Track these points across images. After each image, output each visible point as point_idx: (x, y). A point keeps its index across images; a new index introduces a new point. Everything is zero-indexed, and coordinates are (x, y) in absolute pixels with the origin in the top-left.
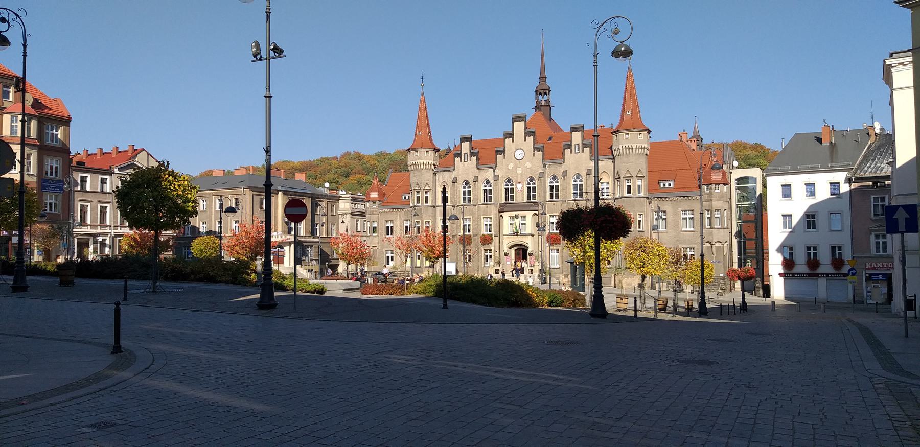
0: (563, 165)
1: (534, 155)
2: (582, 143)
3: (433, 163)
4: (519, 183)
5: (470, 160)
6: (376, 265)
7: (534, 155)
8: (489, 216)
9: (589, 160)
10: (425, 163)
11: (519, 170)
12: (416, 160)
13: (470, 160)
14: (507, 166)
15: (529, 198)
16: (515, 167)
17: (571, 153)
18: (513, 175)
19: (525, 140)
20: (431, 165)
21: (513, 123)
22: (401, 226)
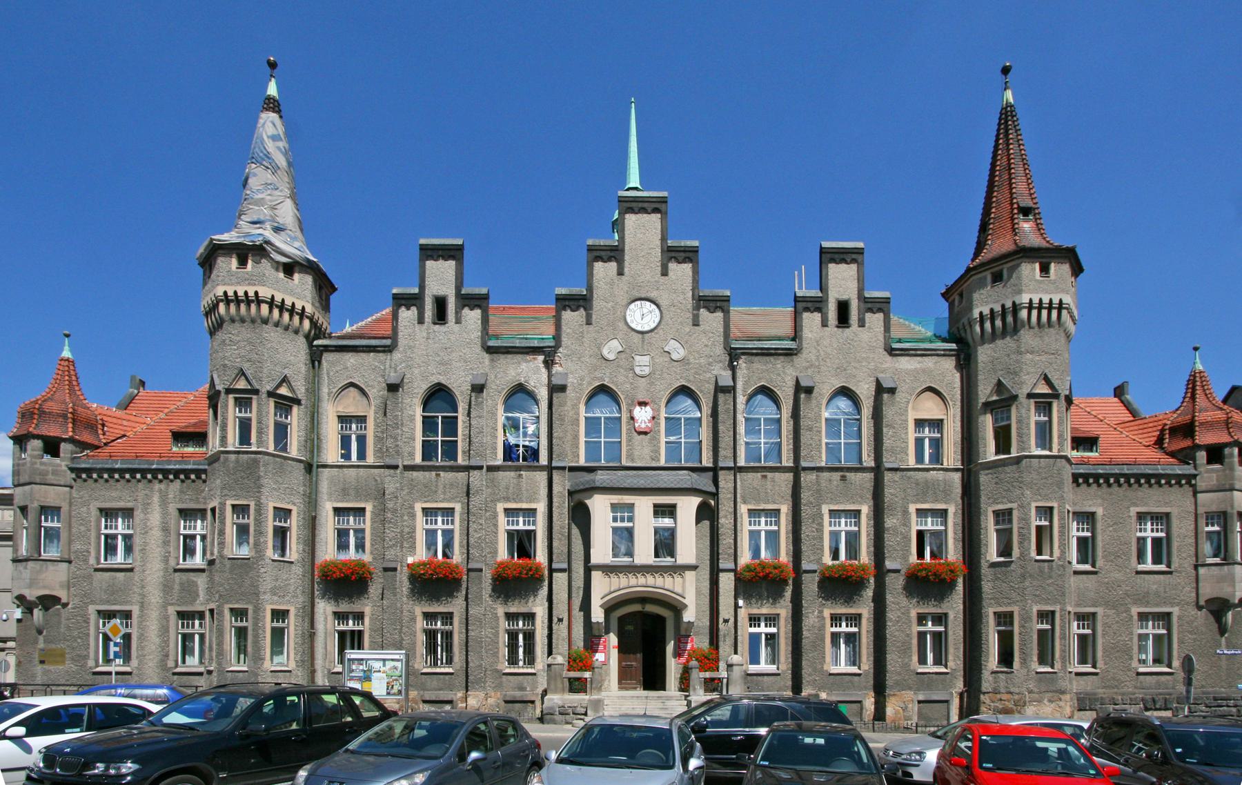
0: (799, 361)
4: (643, 404)
6: (56, 663)
9: (882, 350)
11: (643, 364)
16: (627, 354)
18: (621, 379)
19: (665, 273)
22: (165, 529)
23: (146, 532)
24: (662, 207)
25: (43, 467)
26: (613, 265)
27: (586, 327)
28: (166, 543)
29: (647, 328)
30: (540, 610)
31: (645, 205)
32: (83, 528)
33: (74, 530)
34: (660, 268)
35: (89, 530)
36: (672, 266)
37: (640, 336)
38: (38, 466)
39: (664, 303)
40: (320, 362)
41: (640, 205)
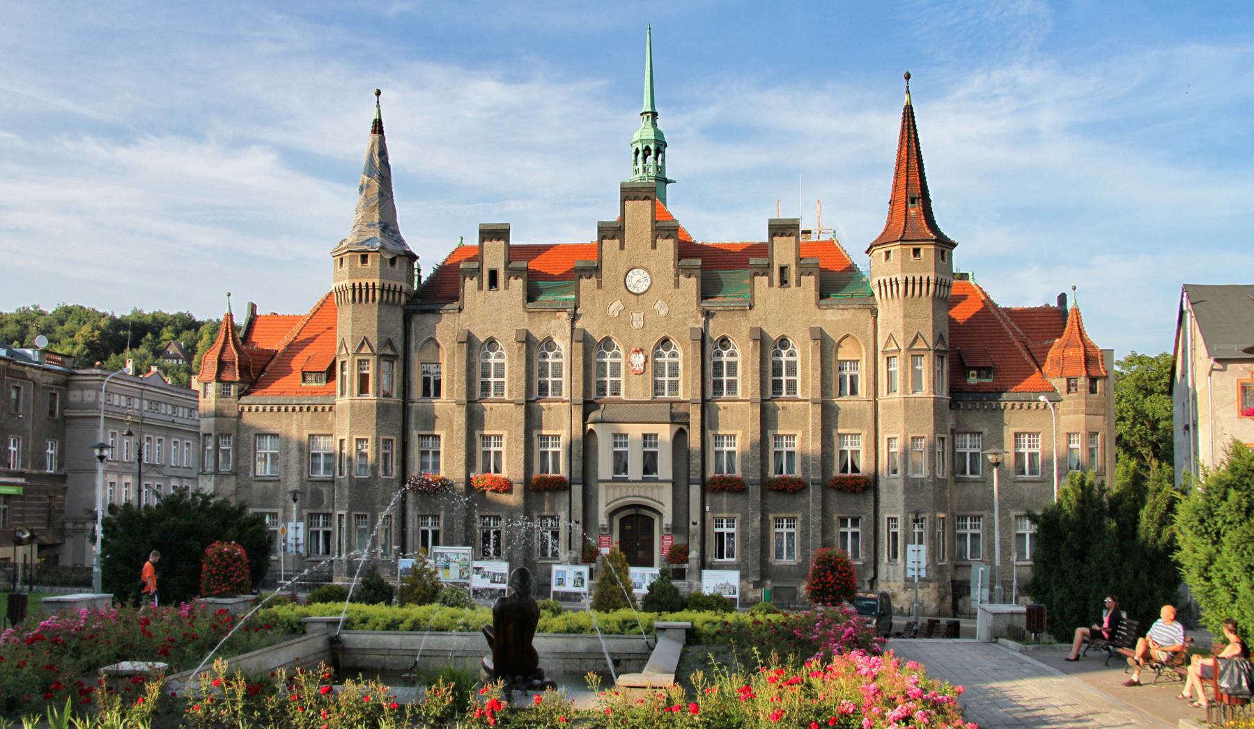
1: (677, 285)
2: (797, 264)
3: (404, 288)
4: (637, 351)
5: (507, 288)
7: (677, 285)
8: (553, 432)
10: (386, 286)
12: (362, 277)
13: (507, 288)
14: (606, 307)
15: (657, 387)
16: (626, 309)
17: (771, 284)
19: (654, 246)
20: (400, 292)
21: (623, 200)
23: (288, 452)
24: (652, 195)
25: (222, 405)
26: (617, 241)
27: (596, 291)
28: (301, 461)
29: (641, 291)
30: (563, 514)
31: (640, 194)
32: (245, 449)
33: (240, 451)
34: (650, 244)
35: (250, 451)
36: (659, 241)
37: (636, 297)
38: (218, 404)
39: (653, 272)
40: (410, 323)
41: (636, 194)
